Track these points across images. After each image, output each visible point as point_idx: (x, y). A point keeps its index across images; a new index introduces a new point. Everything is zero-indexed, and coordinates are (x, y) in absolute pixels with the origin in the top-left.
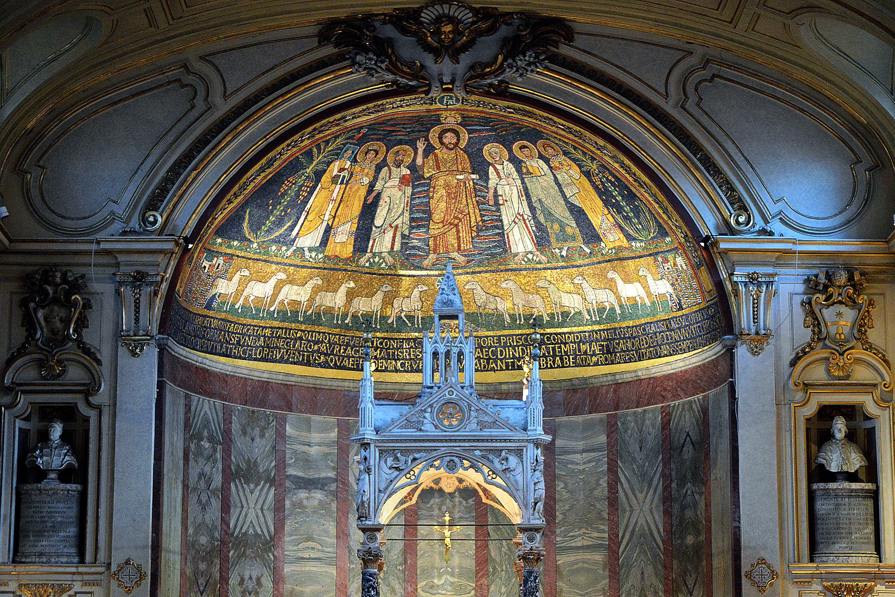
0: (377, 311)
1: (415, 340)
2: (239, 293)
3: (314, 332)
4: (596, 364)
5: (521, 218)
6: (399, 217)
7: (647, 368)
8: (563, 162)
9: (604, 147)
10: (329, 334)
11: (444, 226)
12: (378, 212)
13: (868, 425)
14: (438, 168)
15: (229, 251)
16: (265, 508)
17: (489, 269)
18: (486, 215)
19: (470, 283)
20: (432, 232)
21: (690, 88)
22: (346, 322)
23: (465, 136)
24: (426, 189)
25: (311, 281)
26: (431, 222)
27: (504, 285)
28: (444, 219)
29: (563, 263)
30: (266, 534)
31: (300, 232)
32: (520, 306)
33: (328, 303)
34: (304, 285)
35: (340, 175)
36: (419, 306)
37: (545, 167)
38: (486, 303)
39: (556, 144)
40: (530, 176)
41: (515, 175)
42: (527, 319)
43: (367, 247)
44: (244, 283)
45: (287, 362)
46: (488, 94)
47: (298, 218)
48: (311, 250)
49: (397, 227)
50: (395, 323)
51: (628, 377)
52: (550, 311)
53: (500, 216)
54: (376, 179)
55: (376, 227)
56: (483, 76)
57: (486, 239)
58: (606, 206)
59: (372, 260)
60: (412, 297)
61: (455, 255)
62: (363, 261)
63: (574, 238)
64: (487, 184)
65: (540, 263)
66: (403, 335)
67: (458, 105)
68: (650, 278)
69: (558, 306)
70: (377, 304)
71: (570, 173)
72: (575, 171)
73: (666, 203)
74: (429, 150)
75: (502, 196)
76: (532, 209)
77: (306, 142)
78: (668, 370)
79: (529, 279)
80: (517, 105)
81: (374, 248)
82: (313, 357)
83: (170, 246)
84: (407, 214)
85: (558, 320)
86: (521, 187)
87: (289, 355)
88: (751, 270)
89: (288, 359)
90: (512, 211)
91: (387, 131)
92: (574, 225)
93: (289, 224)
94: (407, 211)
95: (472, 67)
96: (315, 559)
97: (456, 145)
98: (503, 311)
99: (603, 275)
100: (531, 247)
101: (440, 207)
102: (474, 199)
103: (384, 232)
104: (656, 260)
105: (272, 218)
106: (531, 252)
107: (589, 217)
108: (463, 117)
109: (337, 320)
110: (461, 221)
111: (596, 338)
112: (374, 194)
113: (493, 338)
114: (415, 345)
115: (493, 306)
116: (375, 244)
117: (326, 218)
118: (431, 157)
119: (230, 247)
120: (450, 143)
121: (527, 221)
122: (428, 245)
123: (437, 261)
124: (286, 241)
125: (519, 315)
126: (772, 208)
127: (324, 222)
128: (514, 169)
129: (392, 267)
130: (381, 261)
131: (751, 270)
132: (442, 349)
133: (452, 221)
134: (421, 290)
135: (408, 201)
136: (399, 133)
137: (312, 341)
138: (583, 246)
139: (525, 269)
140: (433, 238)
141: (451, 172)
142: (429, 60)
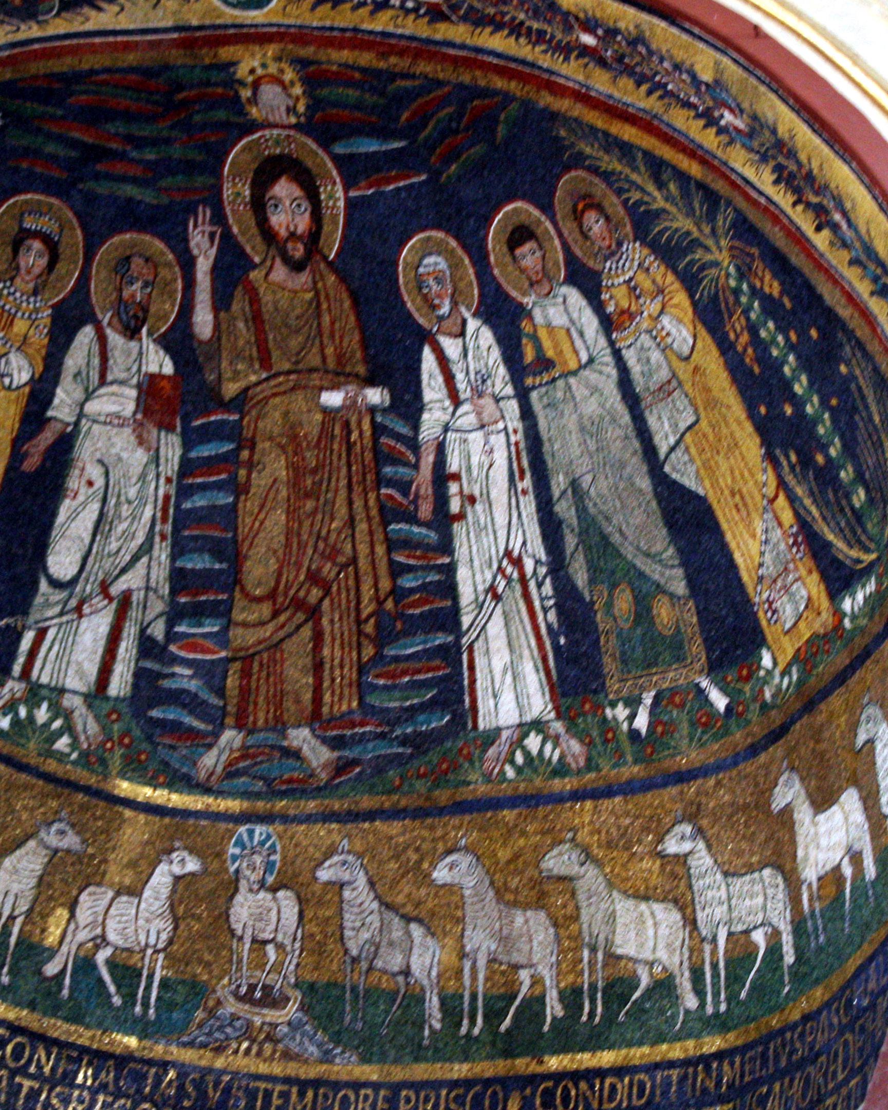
0: (12, 918)
1: (123, 1060)
5: (515, 575)
6: (135, 558)
8: (641, 277)
11: (275, 614)
12: (61, 518)
14: (265, 361)
17: (403, 803)
18: (410, 569)
19: (336, 859)
24: (228, 447)
26: (237, 595)
27: (441, 874)
28: (278, 582)
29: (636, 769)
32: (482, 963)
36: (164, 936)
37: (590, 322)
38: (378, 947)
39: (607, 176)
40: (546, 378)
43: (12, 655)
49: (125, 601)
50: (67, 981)
52: (571, 978)
53: (450, 570)
55: (56, 584)
57: (404, 673)
59: (23, 712)
60: (147, 893)
64: (416, 427)
65: (561, 770)
66: (83, 1036)
69: (600, 956)
70: (15, 888)
75: (456, 477)
79: (522, 842)
84: (162, 553)
85: (592, 1014)
86: (520, 436)
90: (487, 540)
91: (74, 144)
92: (680, 587)
94: (163, 537)
98: (425, 982)
102: (372, 496)
103: (79, 609)
106: (538, 725)
107: (729, 537)
110: (327, 592)
111: (704, 1091)
112: (47, 437)
113: (376, 1095)
114: (117, 1080)
115: (395, 962)
118: (239, 304)
120: (292, 235)
121: (532, 584)
122: (221, 692)
123: (243, 757)
125: (474, 997)
128: (496, 353)
130: (57, 724)
133: (302, 594)
134: (177, 870)
135: (167, 498)
136: (120, 169)
138: (704, 683)
139: (513, 801)
140: (237, 665)
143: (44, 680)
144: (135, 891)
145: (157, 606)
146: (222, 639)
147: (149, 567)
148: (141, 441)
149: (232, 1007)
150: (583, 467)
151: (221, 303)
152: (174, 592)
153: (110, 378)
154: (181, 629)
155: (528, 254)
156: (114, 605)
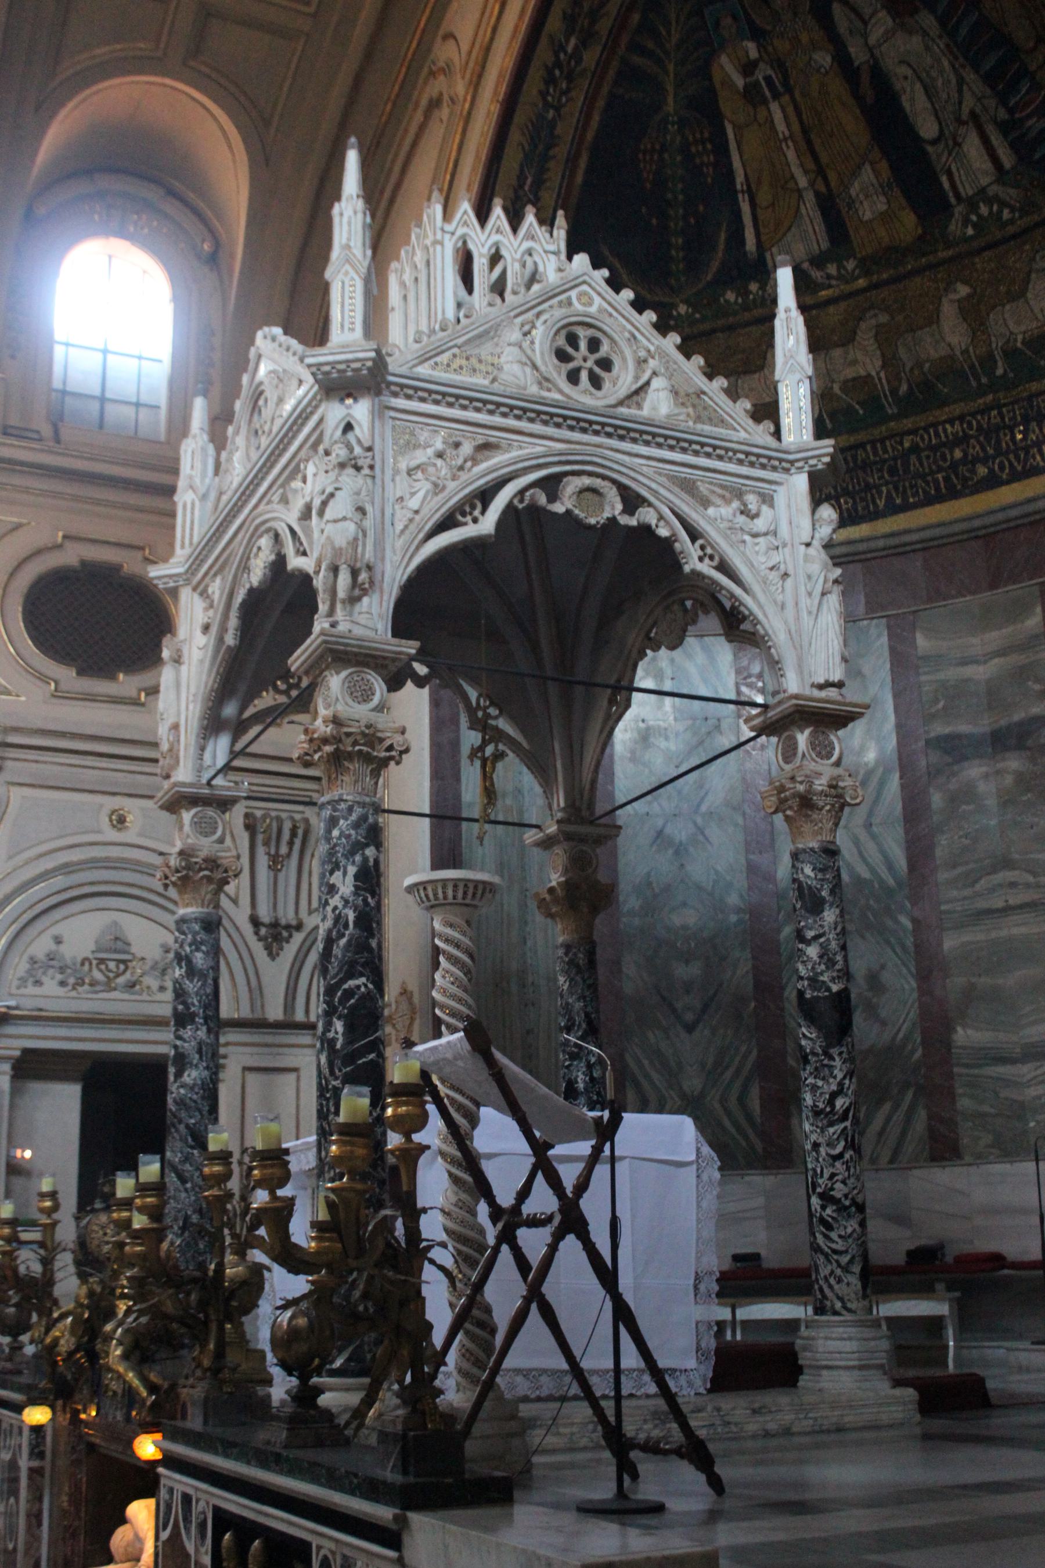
3: (939, 423)
6: (960, 91)
10: (973, 415)
16: (875, 820)
22: (1000, 372)
25: (863, 325)
30: (885, 874)
31: (764, 238)
33: (932, 352)
34: (854, 340)
35: (757, 82)
45: (905, 508)
47: (738, 214)
55: (934, 142)
59: (974, 218)
62: (954, 227)
77: (590, 58)
81: (961, 190)
82: (957, 477)
84: (970, 76)
87: (905, 491)
89: (905, 499)
93: (723, 236)
94: (963, 66)
96: (1021, 907)
103: (958, 144)
109: (978, 379)
112: (865, 78)
116: (957, 178)
117: (803, 182)
127: (804, 194)
130: (995, 208)
135: (947, 46)
137: (944, 445)
143: (970, 193)
145: (991, 103)
147: (970, 89)
148: (910, 33)
152: (992, 88)
153: (867, 17)
154: (1012, 103)
156: (971, 124)
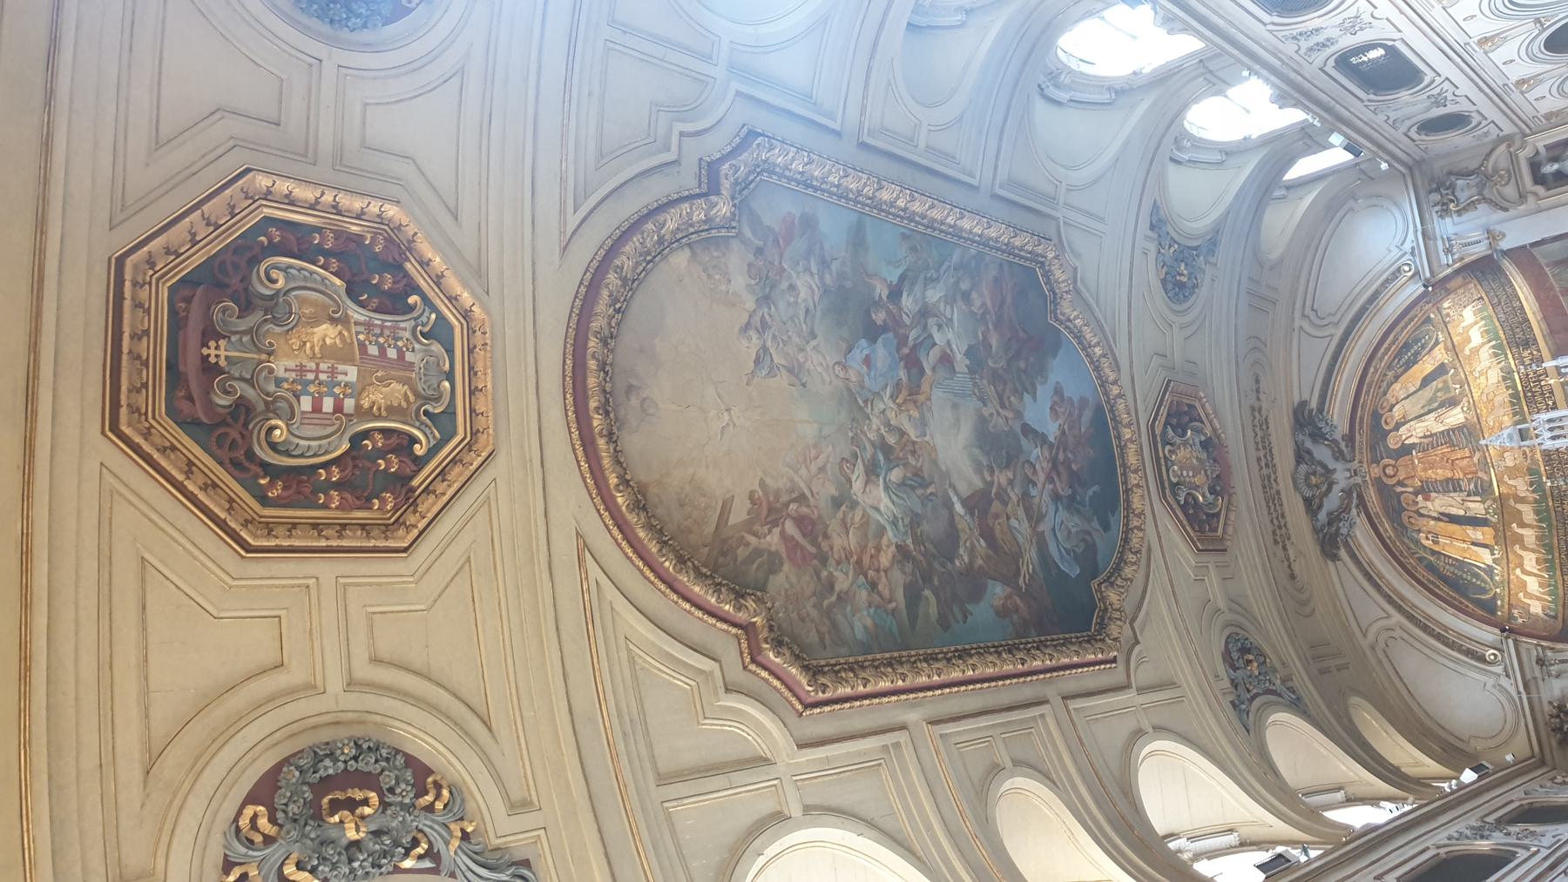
2: (1538, 599)
4: (1539, 351)
7: (1534, 313)
9: (1375, 368)
13: (1543, 151)
15: (1507, 606)
20: (1461, 477)
21: (1325, 322)
23: (1386, 461)
27: (1491, 424)
37: (1397, 407)
41: (1407, 426)
42: (1513, 404)
44: (1529, 595)
46: (1353, 447)
48: (1493, 554)
51: (1544, 326)
54: (1429, 517)
56: (1341, 452)
58: (1417, 362)
61: (1475, 459)
62: (1493, 520)
63: (1445, 382)
65: (1469, 402)
67: (1365, 465)
68: (1463, 325)
71: (1398, 390)
72: (1397, 386)
73: (1406, 319)
74: (1400, 483)
76: (1430, 412)
78: (1532, 298)
80: (1357, 427)
83: (1510, 641)
84: (1452, 494)
88: (1442, 254)
92: (1435, 383)
95: (1337, 459)
97: (1394, 466)
99: (1469, 358)
100: (1458, 409)
101: (1441, 473)
104: (1449, 322)
105: (1474, 580)
108: (1372, 463)
118: (1406, 482)
119: (1502, 606)
124: (1489, 571)
126: (1395, 253)
129: (1494, 500)
131: (1442, 254)
132: (1549, 434)
141: (1414, 468)
142: (1336, 488)
144: (1515, 487)
146: (1463, 480)
149: (1529, 461)
150: (1419, 406)
151: (1406, 486)
155: (1388, 420)
